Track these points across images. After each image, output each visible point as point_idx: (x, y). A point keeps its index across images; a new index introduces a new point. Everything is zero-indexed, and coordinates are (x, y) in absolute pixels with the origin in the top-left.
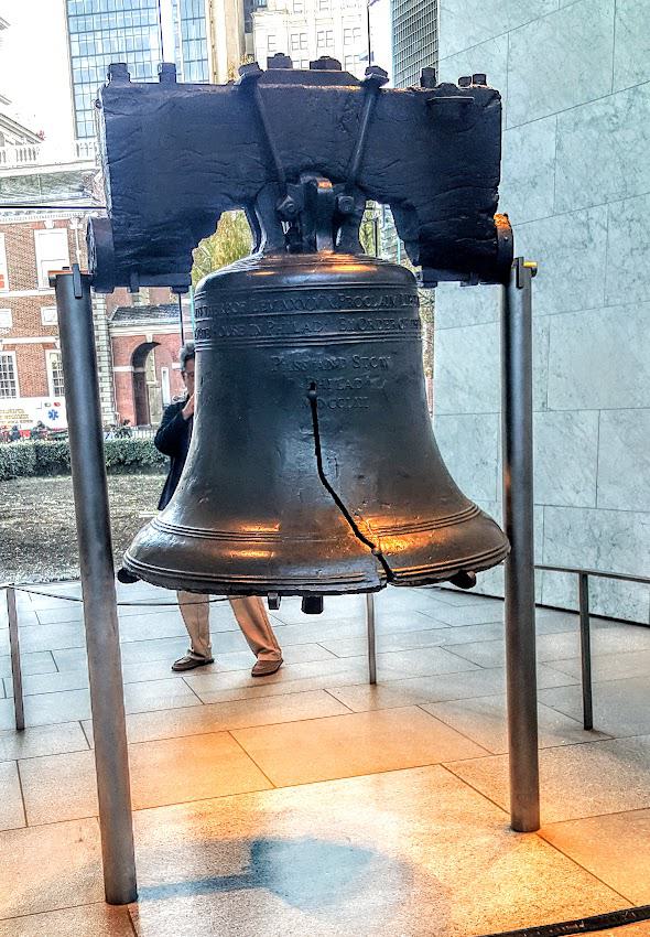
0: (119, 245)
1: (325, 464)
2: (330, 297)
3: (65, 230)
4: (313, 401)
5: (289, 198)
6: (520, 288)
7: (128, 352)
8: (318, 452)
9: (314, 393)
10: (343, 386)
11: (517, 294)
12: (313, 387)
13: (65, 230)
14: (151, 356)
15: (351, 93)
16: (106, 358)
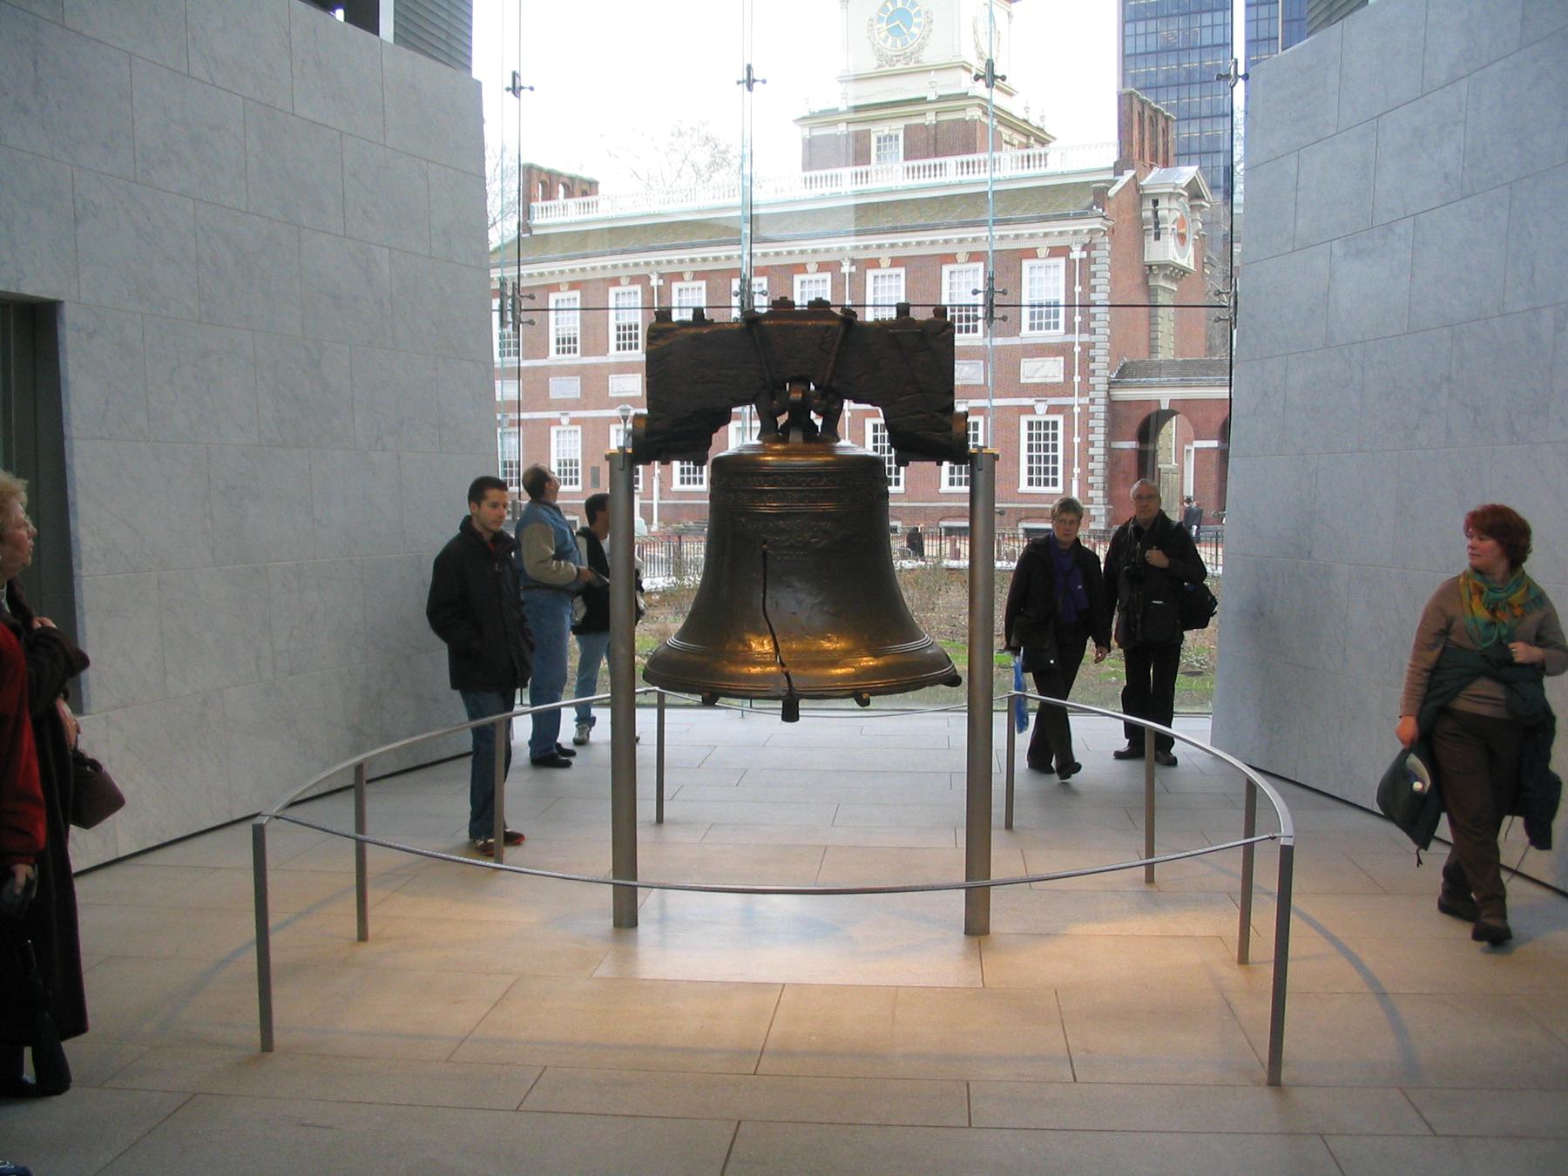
0: (647, 435)
1: (768, 601)
2: (781, 479)
3: (1062, 261)
4: (765, 553)
5: (775, 402)
6: (981, 470)
7: (1134, 426)
8: (765, 593)
9: (765, 546)
10: (787, 544)
11: (981, 476)
12: (765, 543)
13: (1062, 261)
14: (1171, 430)
15: (828, 328)
16: (1102, 430)
